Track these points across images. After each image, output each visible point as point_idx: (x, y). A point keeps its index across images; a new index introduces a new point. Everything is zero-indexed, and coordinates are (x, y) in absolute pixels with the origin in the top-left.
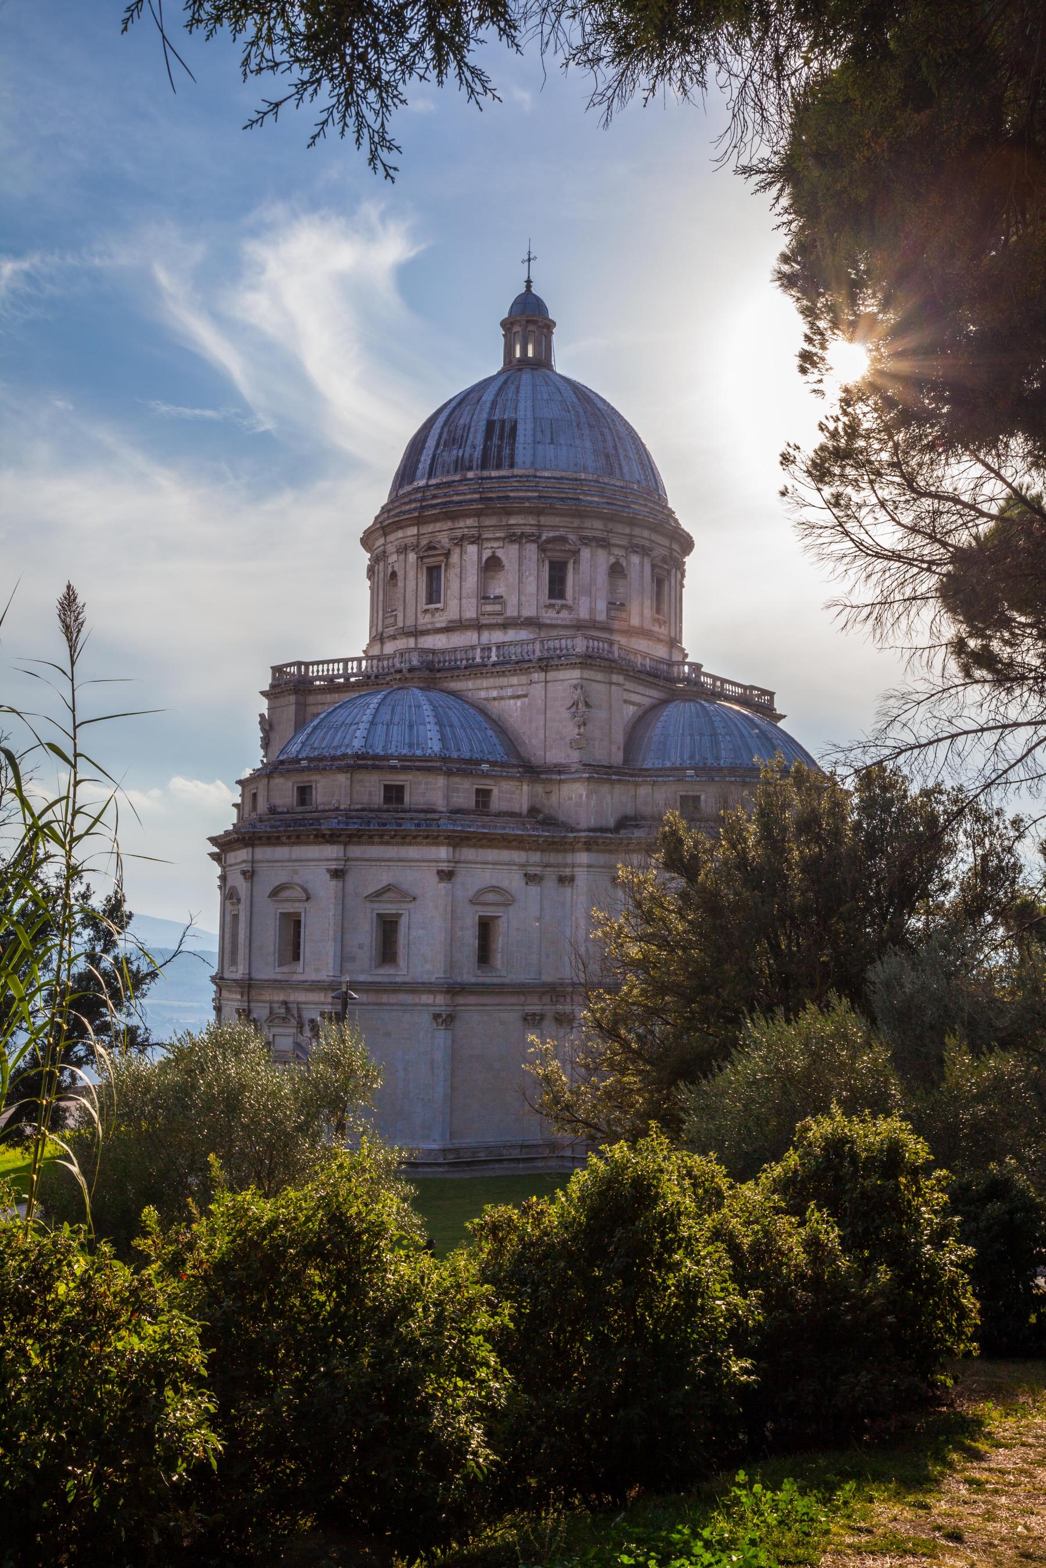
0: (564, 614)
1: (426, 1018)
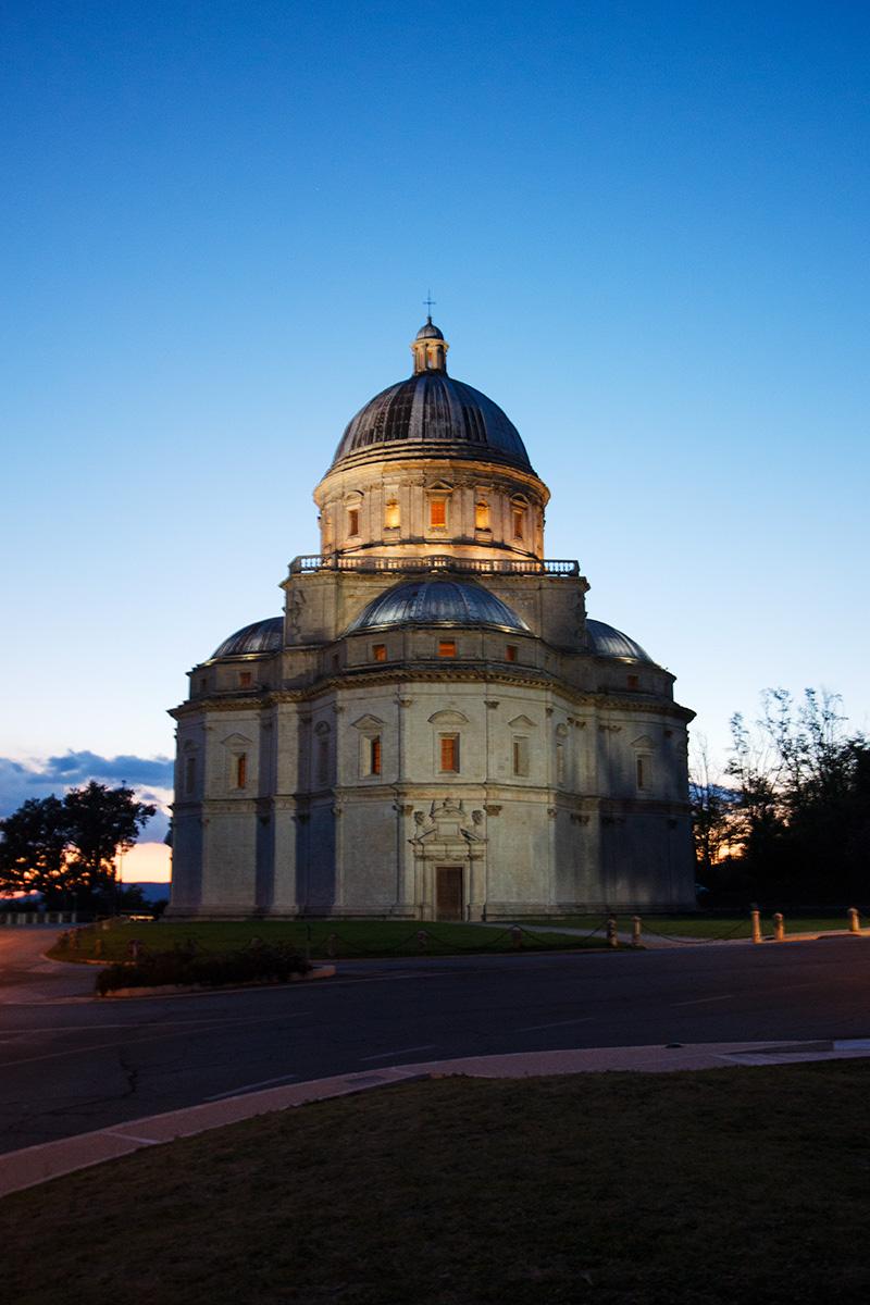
1: (545, 812)
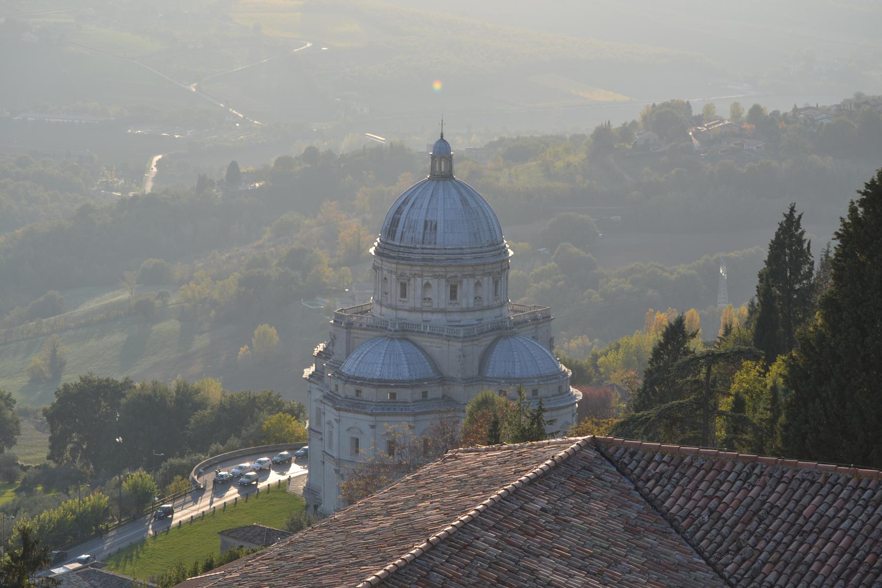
0: (457, 306)
